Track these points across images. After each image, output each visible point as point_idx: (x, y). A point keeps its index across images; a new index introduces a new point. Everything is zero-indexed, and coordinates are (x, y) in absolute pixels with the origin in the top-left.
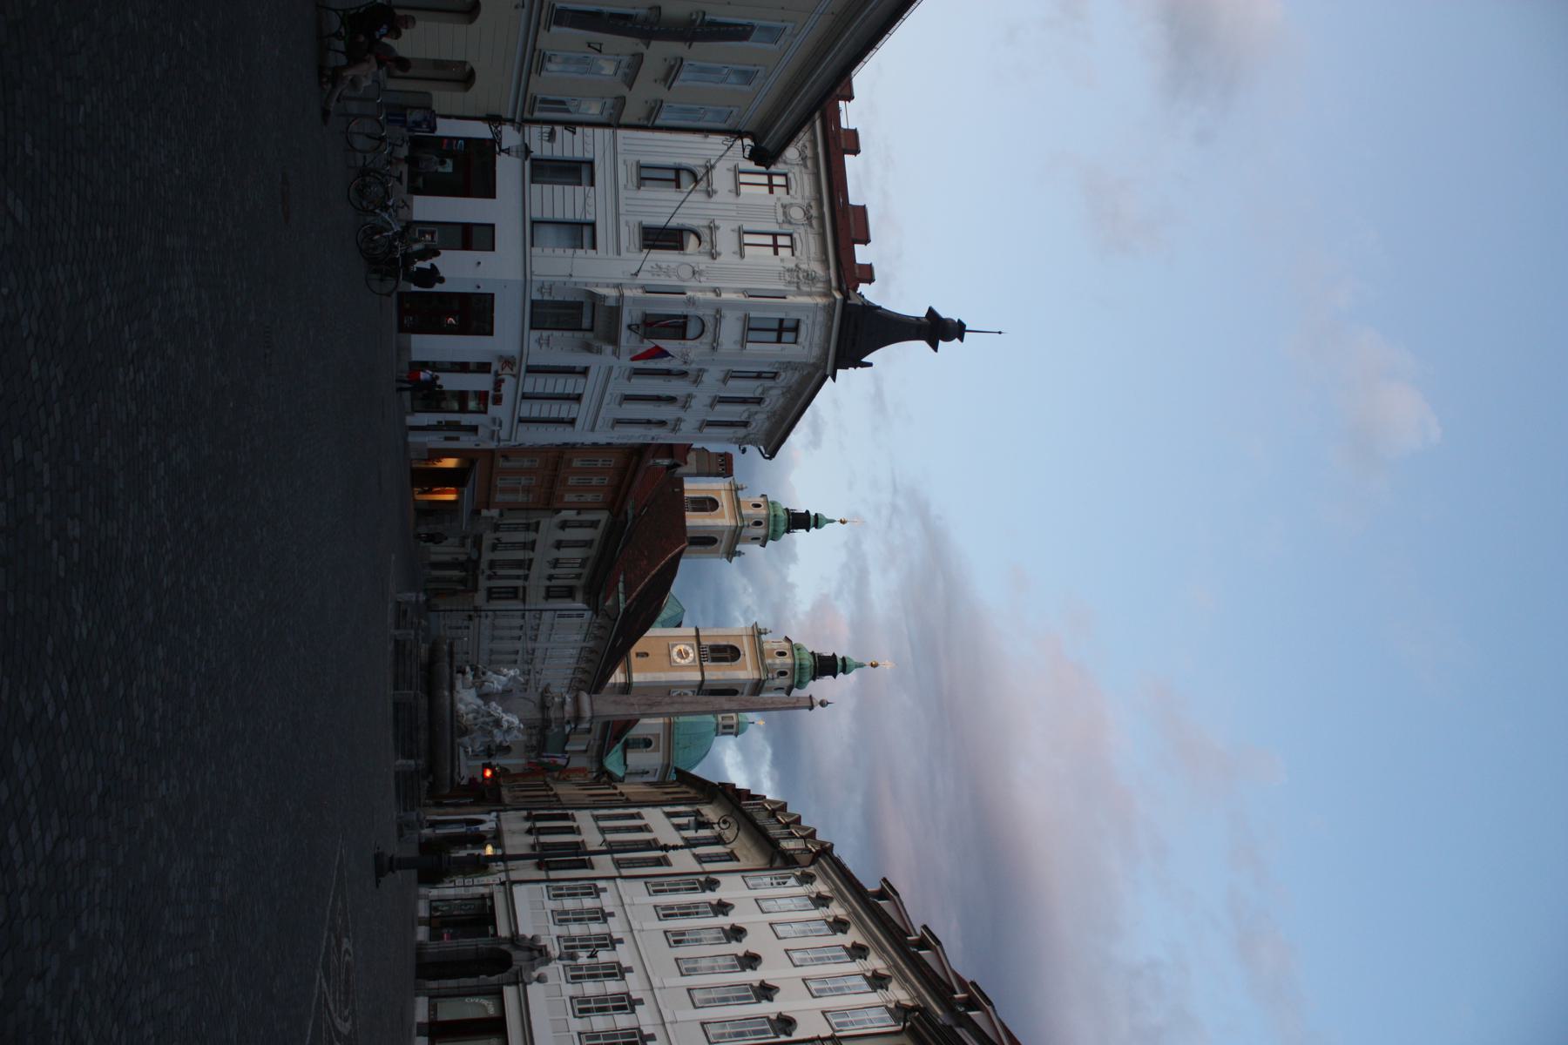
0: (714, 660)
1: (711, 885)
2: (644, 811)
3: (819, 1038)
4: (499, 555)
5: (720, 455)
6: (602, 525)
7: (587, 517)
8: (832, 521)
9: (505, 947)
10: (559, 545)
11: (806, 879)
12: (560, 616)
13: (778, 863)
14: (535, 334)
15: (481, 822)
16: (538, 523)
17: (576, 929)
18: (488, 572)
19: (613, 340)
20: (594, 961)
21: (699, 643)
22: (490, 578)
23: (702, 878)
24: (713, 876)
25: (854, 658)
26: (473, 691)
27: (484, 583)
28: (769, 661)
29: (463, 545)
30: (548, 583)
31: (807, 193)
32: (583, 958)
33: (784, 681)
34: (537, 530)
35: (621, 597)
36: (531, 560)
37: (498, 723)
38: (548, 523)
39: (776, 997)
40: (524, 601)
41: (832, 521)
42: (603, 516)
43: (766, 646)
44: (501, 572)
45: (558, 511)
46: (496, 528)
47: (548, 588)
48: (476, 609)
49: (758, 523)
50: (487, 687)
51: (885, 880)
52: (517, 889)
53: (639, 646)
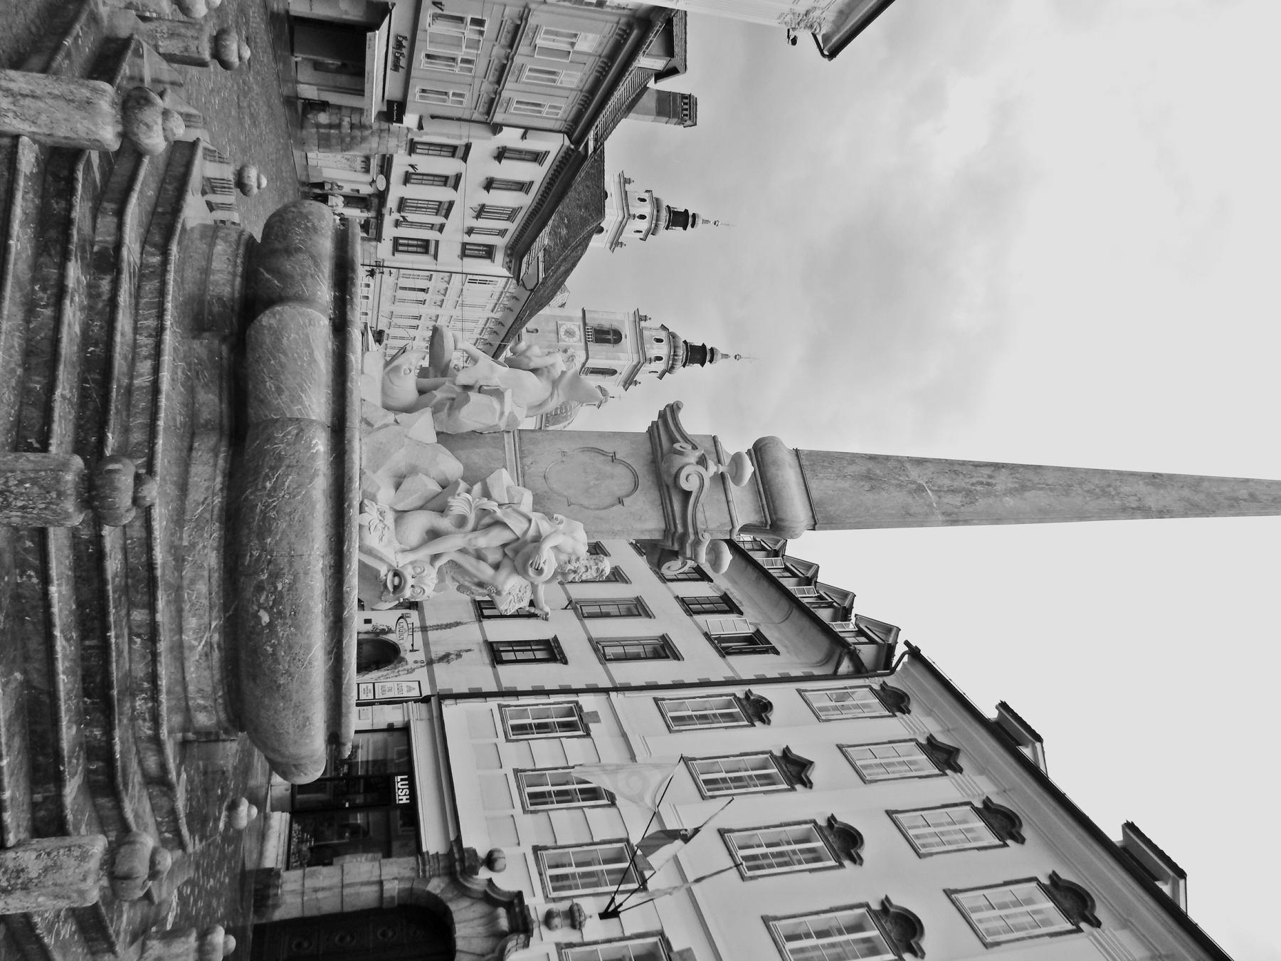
0: (598, 340)
1: (759, 711)
4: (412, 192)
5: (684, 97)
6: (549, 161)
7: (535, 143)
8: (706, 222)
9: (436, 886)
10: (489, 185)
11: (896, 702)
12: (472, 281)
13: (845, 666)
16: (468, 147)
17: (566, 824)
18: (396, 216)
20: (609, 928)
21: (585, 324)
22: (397, 224)
23: (740, 691)
24: (758, 691)
25: (721, 349)
26: (423, 425)
27: (389, 231)
28: (647, 346)
29: (367, 170)
30: (467, 239)
32: (594, 929)
33: (660, 366)
34: (465, 159)
36: (451, 204)
37: (520, 554)
38: (484, 145)
40: (436, 257)
41: (706, 222)
42: (554, 145)
43: (646, 333)
44: (411, 217)
45: (496, 128)
46: (412, 147)
47: (464, 245)
48: (379, 265)
49: (642, 217)
50: (475, 414)
51: (1003, 706)
52: (449, 709)
53: (530, 325)
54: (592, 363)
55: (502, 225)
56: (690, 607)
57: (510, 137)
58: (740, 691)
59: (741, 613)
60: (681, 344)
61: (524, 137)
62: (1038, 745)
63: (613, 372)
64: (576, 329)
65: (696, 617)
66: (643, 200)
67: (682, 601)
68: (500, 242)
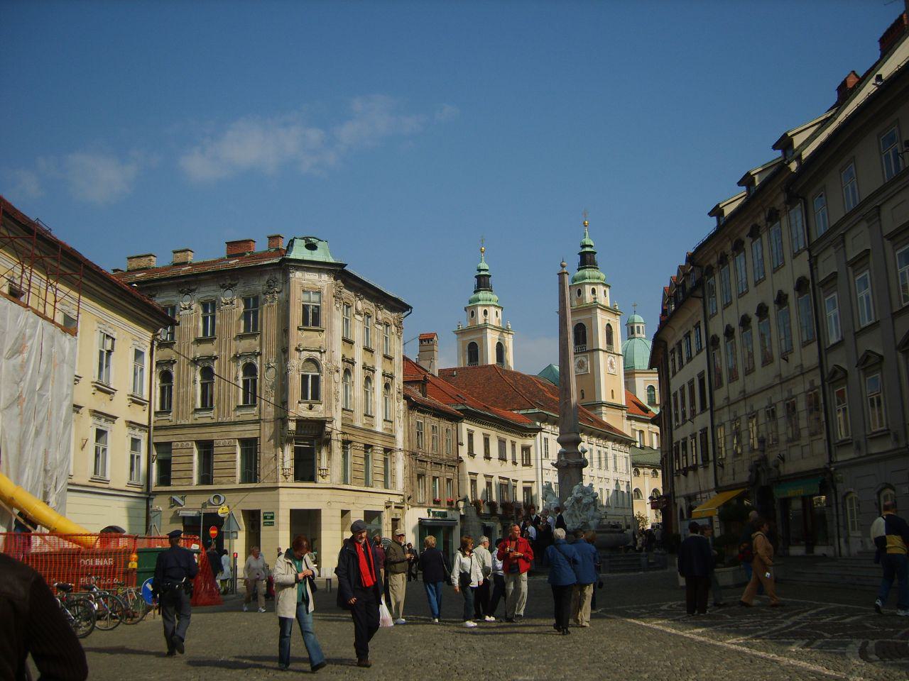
0: (585, 342)
2: (672, 393)
3: (809, 261)
6: (471, 428)
7: (465, 440)
10: (487, 457)
14: (320, 479)
15: (681, 510)
16: (470, 473)
19: (321, 423)
23: (711, 348)
24: (710, 340)
31: (214, 288)
34: (476, 474)
35: (530, 411)
37: (578, 500)
38: (469, 465)
39: (785, 292)
40: (533, 482)
42: (465, 426)
45: (460, 460)
47: (523, 465)
54: (602, 343)
55: (508, 445)
56: (690, 359)
57: (463, 452)
58: (711, 348)
59: (690, 331)
60: (581, 272)
61: (462, 444)
62: (721, 206)
63: (608, 325)
64: (580, 359)
65: (693, 356)
66: (473, 312)
67: (688, 362)
68: (520, 442)
